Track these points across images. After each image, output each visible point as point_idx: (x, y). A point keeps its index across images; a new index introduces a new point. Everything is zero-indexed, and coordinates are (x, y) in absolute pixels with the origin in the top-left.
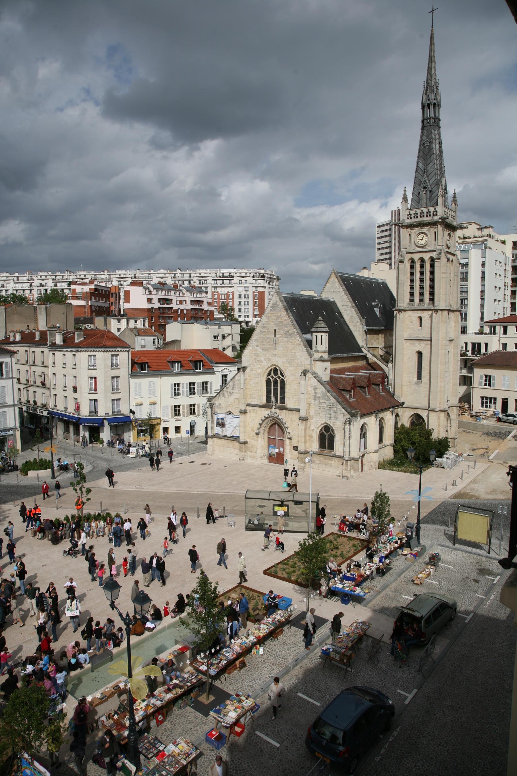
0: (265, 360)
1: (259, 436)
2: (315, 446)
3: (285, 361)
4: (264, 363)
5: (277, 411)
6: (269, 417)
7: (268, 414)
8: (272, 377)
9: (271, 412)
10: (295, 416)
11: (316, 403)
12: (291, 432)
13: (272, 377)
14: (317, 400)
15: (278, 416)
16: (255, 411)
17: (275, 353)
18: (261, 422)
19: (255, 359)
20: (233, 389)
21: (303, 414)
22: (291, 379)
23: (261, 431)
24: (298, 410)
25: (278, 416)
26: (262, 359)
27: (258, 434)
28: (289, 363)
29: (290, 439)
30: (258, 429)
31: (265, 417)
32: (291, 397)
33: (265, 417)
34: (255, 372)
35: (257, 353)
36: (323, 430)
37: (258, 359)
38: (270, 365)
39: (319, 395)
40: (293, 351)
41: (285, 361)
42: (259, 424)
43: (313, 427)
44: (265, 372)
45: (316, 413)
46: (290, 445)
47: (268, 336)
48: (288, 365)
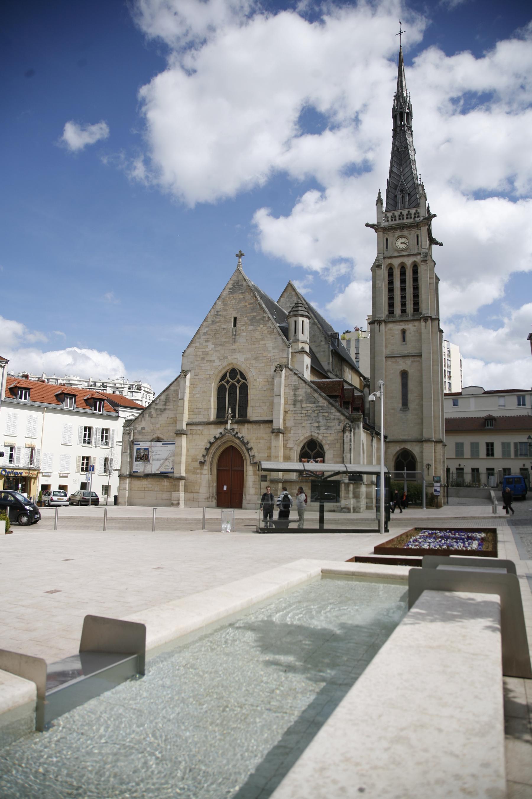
0: (218, 358)
1: (205, 467)
4: (217, 363)
5: (235, 426)
7: (221, 433)
8: (228, 382)
9: (225, 429)
12: (256, 454)
13: (228, 382)
14: (298, 405)
15: (237, 433)
16: (199, 432)
17: (233, 347)
18: (208, 446)
19: (203, 359)
20: (165, 405)
22: (258, 380)
23: (208, 459)
25: (237, 433)
26: (214, 357)
27: (202, 463)
30: (204, 456)
31: (215, 437)
32: (257, 405)
33: (215, 437)
34: (202, 377)
35: (207, 350)
36: (306, 447)
37: (206, 359)
39: (300, 398)
40: (261, 342)
42: (206, 449)
43: (290, 444)
45: (296, 423)
47: (224, 326)
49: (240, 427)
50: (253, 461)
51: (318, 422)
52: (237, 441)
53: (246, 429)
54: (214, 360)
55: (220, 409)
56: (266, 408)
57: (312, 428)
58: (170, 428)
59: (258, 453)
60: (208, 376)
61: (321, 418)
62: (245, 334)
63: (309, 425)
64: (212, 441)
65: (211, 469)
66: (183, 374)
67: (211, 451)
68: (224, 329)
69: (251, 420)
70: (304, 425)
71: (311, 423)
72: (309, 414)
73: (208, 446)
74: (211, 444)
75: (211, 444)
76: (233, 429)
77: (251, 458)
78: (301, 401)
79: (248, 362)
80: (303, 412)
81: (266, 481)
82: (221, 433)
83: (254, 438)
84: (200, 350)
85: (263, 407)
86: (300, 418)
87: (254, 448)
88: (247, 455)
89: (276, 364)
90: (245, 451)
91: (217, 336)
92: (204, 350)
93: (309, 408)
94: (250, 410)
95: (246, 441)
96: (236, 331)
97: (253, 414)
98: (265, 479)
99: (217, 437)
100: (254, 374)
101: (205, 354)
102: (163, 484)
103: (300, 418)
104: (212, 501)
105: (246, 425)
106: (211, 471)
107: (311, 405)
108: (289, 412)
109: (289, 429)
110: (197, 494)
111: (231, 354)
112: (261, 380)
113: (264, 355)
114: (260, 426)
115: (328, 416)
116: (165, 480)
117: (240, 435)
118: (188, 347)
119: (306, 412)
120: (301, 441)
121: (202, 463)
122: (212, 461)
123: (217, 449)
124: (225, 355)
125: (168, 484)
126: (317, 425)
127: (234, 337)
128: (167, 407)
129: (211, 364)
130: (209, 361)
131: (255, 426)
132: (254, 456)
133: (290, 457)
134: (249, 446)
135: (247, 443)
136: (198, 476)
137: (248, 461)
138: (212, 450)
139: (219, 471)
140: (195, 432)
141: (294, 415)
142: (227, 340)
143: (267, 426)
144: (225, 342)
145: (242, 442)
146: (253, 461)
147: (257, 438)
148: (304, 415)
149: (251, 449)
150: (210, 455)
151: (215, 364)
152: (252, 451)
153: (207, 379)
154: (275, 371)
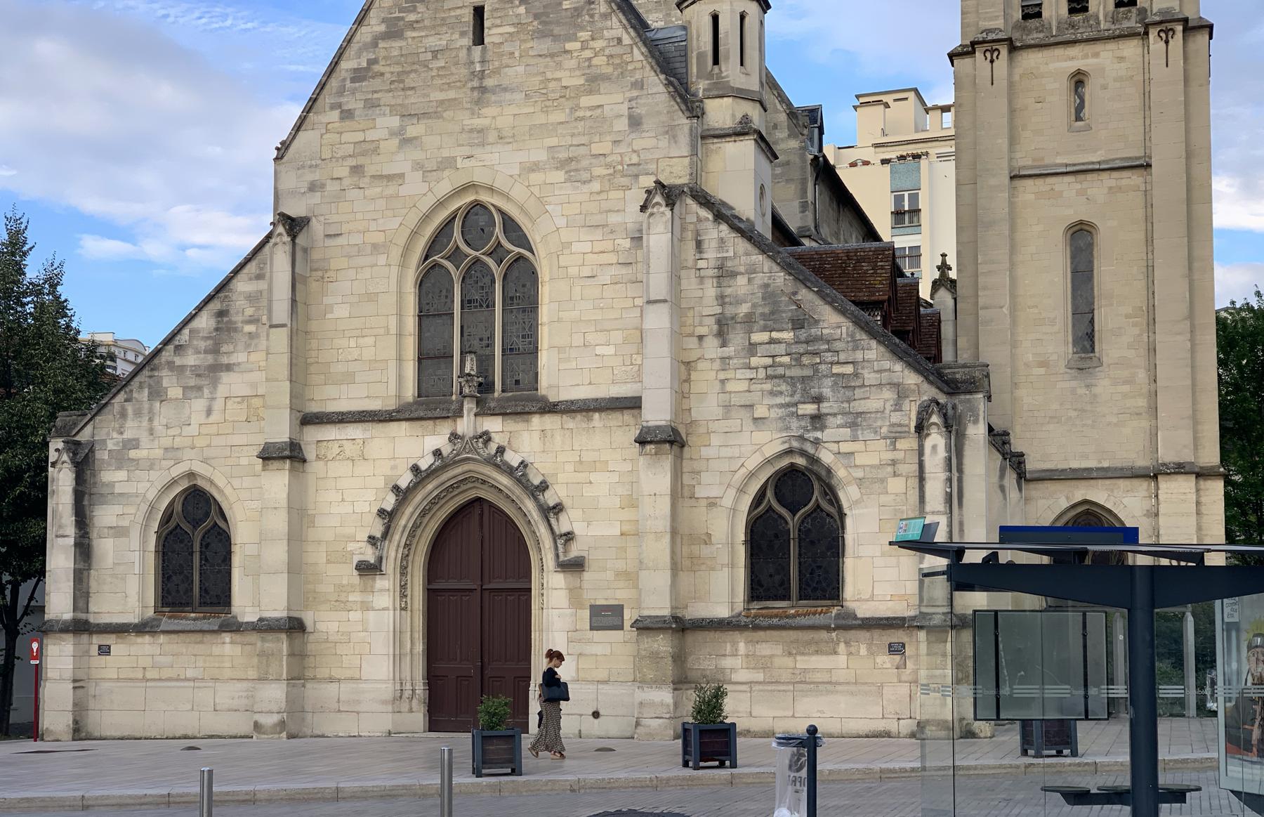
0: (418, 166)
1: (381, 583)
2: (724, 590)
3: (542, 156)
4: (414, 186)
5: (493, 425)
6: (444, 467)
7: (437, 453)
8: (456, 255)
9: (454, 437)
10: (611, 440)
11: (729, 351)
12: (578, 529)
13: (456, 255)
14: (737, 338)
15: (501, 450)
16: (349, 449)
17: (478, 122)
18: (390, 502)
19: (357, 170)
21: (657, 413)
22: (576, 247)
23: (392, 552)
24: (632, 404)
25: (501, 450)
26: (401, 163)
27: (368, 569)
28: (563, 164)
29: (575, 566)
30: (372, 540)
31: (415, 469)
32: (578, 340)
33: (415, 469)
34: (356, 239)
35: (371, 135)
36: (770, 494)
37: (371, 170)
38: (444, 188)
39: (744, 309)
40: (585, 101)
41: (542, 156)
42: (381, 512)
43: (709, 486)
44: (415, 234)
45: (727, 407)
46: (575, 596)
47: (433, 42)
48: (560, 176)
49: (513, 425)
50: (565, 552)
51: (818, 400)
52: (504, 481)
53: (536, 435)
54: (402, 176)
55: (431, 357)
56: (610, 350)
57: (795, 424)
58: (237, 440)
59: (591, 525)
60: (379, 238)
61: (828, 382)
62: (521, 69)
63: (781, 412)
64: (403, 484)
65: (403, 587)
66: (280, 229)
67: (403, 522)
68: (435, 54)
69: (553, 398)
70: (760, 411)
71: (788, 405)
72: (780, 371)
73: (390, 502)
74: (403, 495)
75: (403, 495)
76: (486, 437)
77: (560, 542)
78: (749, 320)
79: (536, 178)
80: (755, 361)
81: (621, 628)
82: (437, 453)
83: (570, 467)
84: (347, 137)
85: (599, 350)
86: (743, 386)
87: (567, 503)
88: (543, 531)
89: (649, 182)
90: (535, 515)
91: (409, 82)
92: (359, 136)
93: (781, 349)
94: (545, 359)
95: (536, 482)
96: (483, 62)
97: (557, 374)
98: (616, 622)
99: (424, 465)
100: (561, 222)
101: (364, 154)
102: (216, 650)
103: (743, 386)
104: (411, 711)
105: (536, 419)
106: (403, 596)
107: (787, 335)
108: (701, 365)
109: (702, 430)
110: (352, 685)
111: (466, 151)
112: (587, 247)
113: (596, 149)
114: (590, 419)
115: (856, 375)
116: (227, 637)
117: (513, 459)
118: (298, 128)
119: (769, 361)
120: (752, 475)
121: (368, 569)
122: (405, 557)
123: (423, 514)
124: (446, 153)
125: (238, 649)
126: (810, 409)
127: (475, 83)
128: (225, 360)
129: (391, 190)
130: (381, 177)
131: (570, 422)
132: (569, 537)
133: (709, 535)
134: (550, 498)
135: (544, 487)
136: (355, 616)
137: (544, 557)
138: (405, 519)
139: (433, 595)
140: (336, 450)
141: (722, 376)
142: (452, 94)
143: (615, 419)
144: (442, 102)
145: (523, 482)
146: (565, 552)
147: (580, 465)
148: (762, 374)
149: (558, 509)
150: (398, 537)
151: (405, 190)
152: (563, 517)
153: (375, 247)
154: (643, 208)
